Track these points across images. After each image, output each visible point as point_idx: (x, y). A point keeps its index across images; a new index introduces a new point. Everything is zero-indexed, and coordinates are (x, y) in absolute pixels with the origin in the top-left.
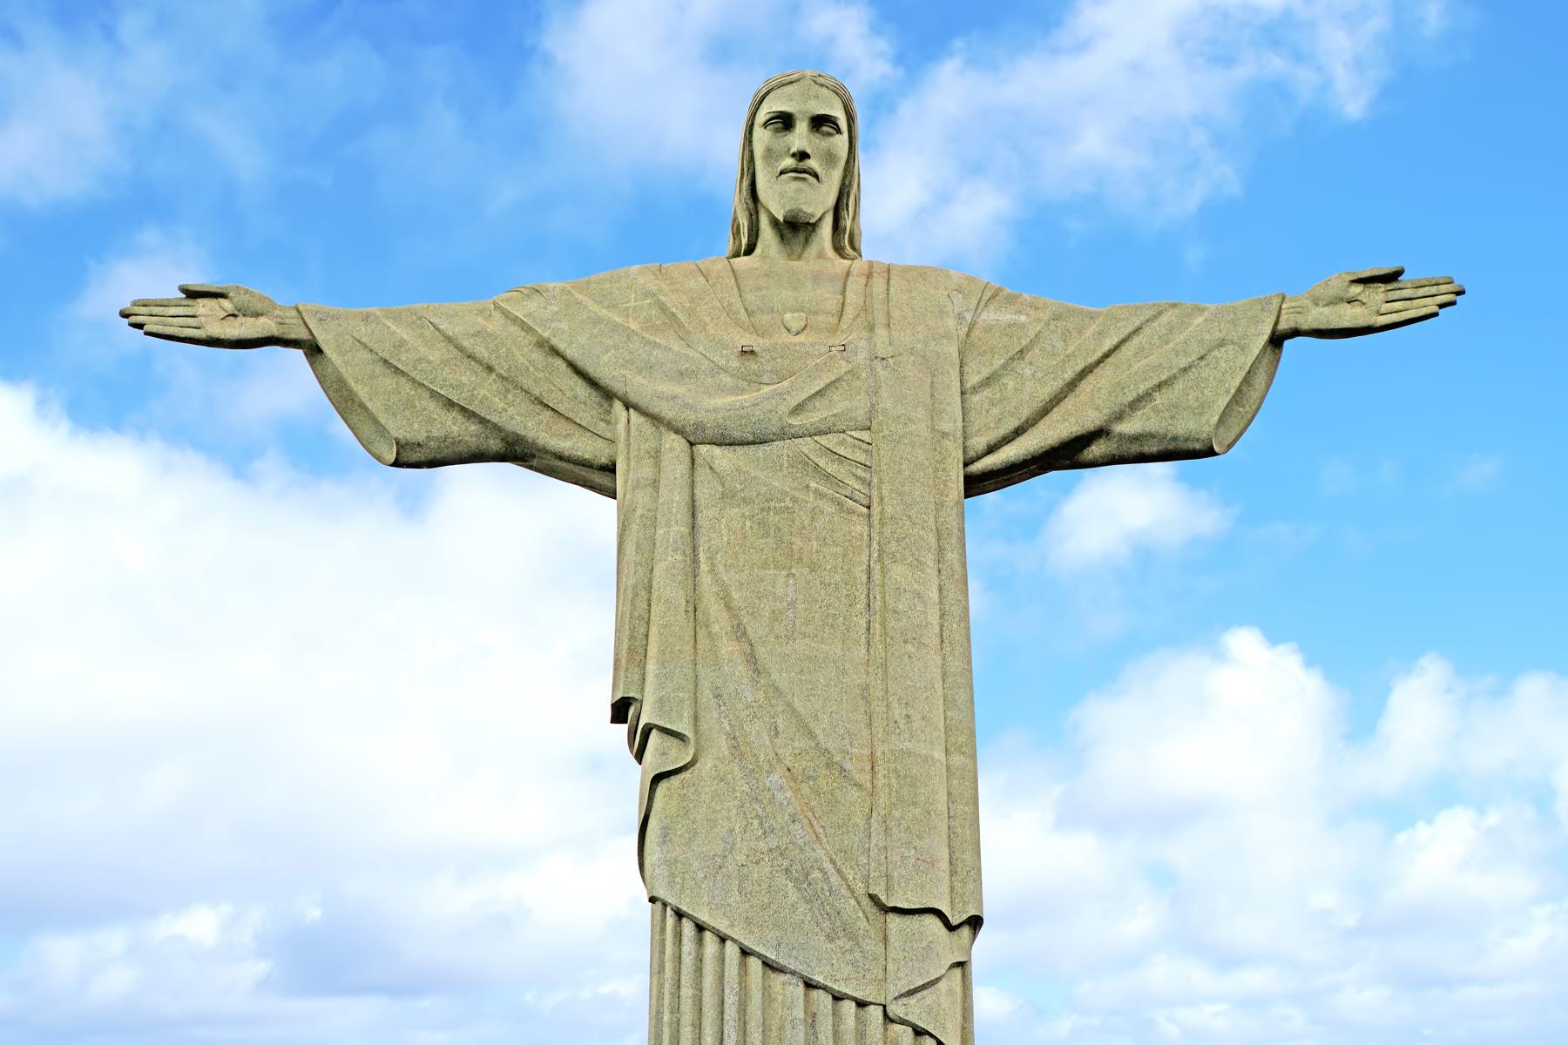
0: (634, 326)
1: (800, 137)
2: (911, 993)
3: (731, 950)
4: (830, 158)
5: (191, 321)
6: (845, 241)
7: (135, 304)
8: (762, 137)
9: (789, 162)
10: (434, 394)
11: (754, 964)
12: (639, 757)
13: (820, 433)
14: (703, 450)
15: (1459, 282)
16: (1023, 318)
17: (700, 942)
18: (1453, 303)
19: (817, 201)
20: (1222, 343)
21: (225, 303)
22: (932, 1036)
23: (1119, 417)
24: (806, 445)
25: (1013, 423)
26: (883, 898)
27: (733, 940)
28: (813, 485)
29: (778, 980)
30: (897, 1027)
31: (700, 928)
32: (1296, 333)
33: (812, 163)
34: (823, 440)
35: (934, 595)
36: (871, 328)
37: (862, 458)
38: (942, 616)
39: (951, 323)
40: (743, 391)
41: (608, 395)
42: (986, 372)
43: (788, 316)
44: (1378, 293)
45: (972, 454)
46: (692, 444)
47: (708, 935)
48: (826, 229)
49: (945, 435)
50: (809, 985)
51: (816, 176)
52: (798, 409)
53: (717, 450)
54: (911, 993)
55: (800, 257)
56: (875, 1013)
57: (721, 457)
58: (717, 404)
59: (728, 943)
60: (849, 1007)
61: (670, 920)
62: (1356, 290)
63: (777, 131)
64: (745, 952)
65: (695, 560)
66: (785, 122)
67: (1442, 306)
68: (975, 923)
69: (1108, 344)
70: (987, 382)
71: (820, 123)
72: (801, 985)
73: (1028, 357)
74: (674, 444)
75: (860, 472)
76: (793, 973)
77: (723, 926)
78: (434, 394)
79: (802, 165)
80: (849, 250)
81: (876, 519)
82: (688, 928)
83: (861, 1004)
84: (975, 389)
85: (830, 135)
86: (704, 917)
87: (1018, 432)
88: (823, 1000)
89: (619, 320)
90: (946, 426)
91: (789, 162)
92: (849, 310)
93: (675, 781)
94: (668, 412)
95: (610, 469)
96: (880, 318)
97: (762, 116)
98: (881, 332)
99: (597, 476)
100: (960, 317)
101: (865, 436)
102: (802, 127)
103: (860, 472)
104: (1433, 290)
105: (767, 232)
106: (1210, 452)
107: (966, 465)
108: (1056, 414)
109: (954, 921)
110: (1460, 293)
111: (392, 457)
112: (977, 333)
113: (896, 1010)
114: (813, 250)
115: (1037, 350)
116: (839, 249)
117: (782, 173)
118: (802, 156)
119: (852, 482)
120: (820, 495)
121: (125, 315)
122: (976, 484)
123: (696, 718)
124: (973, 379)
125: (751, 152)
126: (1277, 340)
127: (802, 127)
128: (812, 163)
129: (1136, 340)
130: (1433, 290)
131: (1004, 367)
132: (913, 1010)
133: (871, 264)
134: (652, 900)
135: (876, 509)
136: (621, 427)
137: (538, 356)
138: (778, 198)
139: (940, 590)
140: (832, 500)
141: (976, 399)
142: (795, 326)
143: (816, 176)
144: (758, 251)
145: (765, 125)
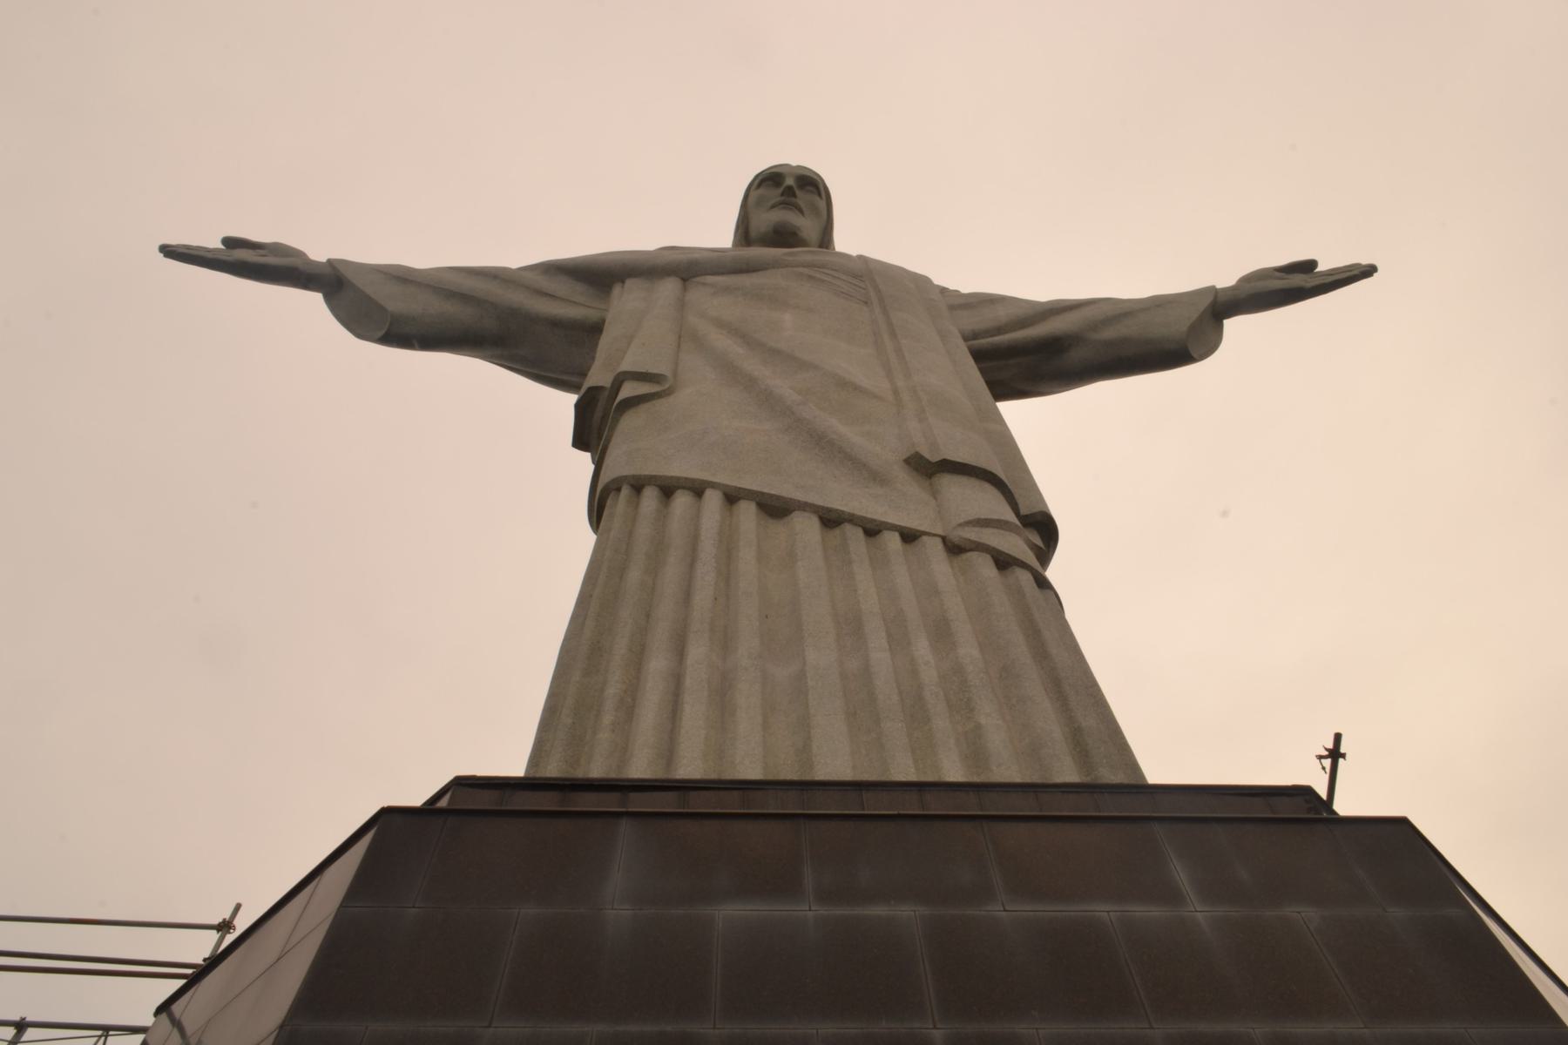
3: (713, 499)
4: (815, 209)
11: (747, 510)
19: (806, 225)
26: (927, 455)
27: (713, 485)
29: (778, 528)
30: (973, 556)
31: (668, 490)
46: (684, 280)
47: (679, 493)
50: (831, 520)
51: (801, 211)
56: (934, 548)
59: (709, 493)
60: (893, 541)
64: (732, 497)
83: (909, 537)
88: (855, 534)
91: (780, 199)
93: (644, 407)
111: (381, 333)
118: (789, 191)
123: (675, 374)
143: (801, 211)
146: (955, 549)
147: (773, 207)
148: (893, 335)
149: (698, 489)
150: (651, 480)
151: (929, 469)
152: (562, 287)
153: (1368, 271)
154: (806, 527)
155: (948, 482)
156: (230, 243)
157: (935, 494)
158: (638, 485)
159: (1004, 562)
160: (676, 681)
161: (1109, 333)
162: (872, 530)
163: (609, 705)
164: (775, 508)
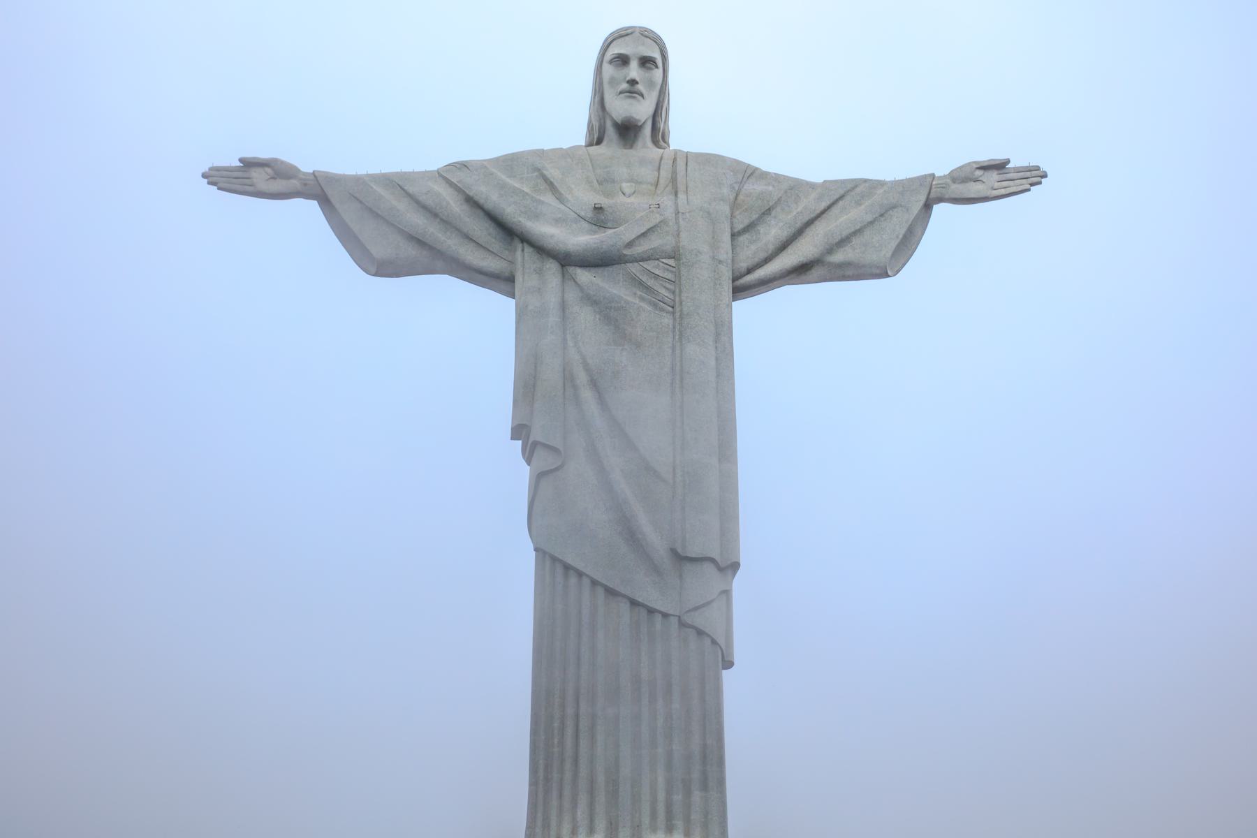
0: (526, 189)
1: (634, 71)
2: (696, 609)
3: (586, 581)
4: (651, 84)
5: (247, 181)
6: (659, 136)
7: (211, 169)
8: (608, 70)
9: (625, 86)
10: (401, 232)
11: (600, 591)
12: (529, 462)
13: (643, 260)
14: (571, 269)
15: (1044, 167)
16: (771, 188)
17: (566, 576)
18: (1040, 183)
20: (893, 207)
21: (268, 170)
22: (708, 636)
23: (830, 251)
24: (634, 268)
25: (762, 255)
26: (679, 551)
28: (639, 293)
31: (567, 568)
32: (940, 200)
33: (640, 87)
34: (647, 265)
35: (713, 363)
36: (676, 194)
37: (670, 276)
38: (718, 376)
39: (725, 191)
40: (595, 232)
41: (509, 233)
42: (747, 222)
43: (624, 185)
44: (994, 176)
45: (737, 274)
46: (563, 266)
47: (572, 572)
48: (647, 130)
49: (720, 262)
50: (634, 603)
51: (642, 95)
52: (630, 244)
53: (579, 271)
54: (696, 609)
55: (631, 147)
56: (674, 621)
57: (583, 276)
58: (579, 239)
60: (658, 618)
61: (548, 563)
62: (979, 173)
63: (617, 66)
64: (594, 583)
65: (565, 340)
66: (623, 60)
67: (1032, 185)
68: (735, 566)
69: (823, 205)
70: (747, 229)
71: (646, 62)
72: (628, 604)
73: (773, 213)
74: (552, 267)
75: (668, 285)
76: (624, 596)
77: (579, 565)
78: (401, 232)
79: (632, 89)
80: (662, 143)
81: (678, 315)
82: (559, 570)
83: (665, 616)
84: (740, 233)
85: (650, 69)
86: (569, 560)
87: (767, 260)
88: (644, 612)
89: (517, 185)
90: (723, 257)
91: (625, 86)
92: (662, 181)
94: (550, 244)
95: (511, 280)
96: (681, 187)
97: (608, 56)
98: (681, 196)
99: (503, 282)
100: (732, 187)
101: (671, 262)
102: (634, 64)
103: (668, 285)
104: (1028, 174)
105: (611, 132)
106: (884, 274)
107: (734, 281)
108: (790, 250)
109: (722, 565)
110: (1045, 176)
111: (373, 270)
112: (741, 197)
113: (688, 619)
114: (639, 143)
115: (778, 209)
116: (655, 142)
117: (621, 93)
118: (633, 82)
119: (663, 291)
120: (642, 299)
121: (204, 176)
122: (740, 290)
124: (739, 227)
125: (601, 79)
126: (928, 207)
127: (634, 64)
128: (640, 87)
129: (841, 202)
130: (1028, 174)
131: (759, 219)
132: (698, 620)
133: (676, 152)
134: (536, 550)
135: (678, 309)
136: (519, 253)
137: (465, 207)
138: (620, 108)
139: (717, 359)
140: (650, 303)
141: (741, 239)
142: (627, 191)
143: (642, 95)
144: (605, 142)
145: (611, 62)
146: (682, 624)
147: (621, 93)
148: (682, 380)
149: (580, 574)
150: (560, 561)
151: (681, 559)
152: (479, 228)
153: (1034, 176)
154: (625, 607)
155: (688, 567)
156: (248, 164)
157: (681, 576)
158: (554, 559)
159: (700, 633)
160: (577, 716)
161: (838, 257)
162: (651, 611)
163: (556, 732)
164: (611, 592)
